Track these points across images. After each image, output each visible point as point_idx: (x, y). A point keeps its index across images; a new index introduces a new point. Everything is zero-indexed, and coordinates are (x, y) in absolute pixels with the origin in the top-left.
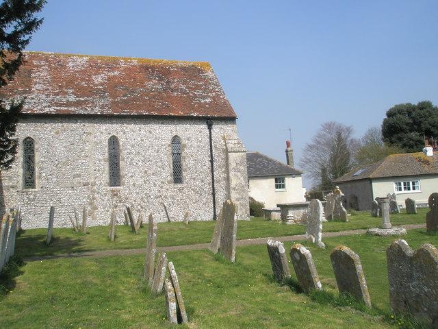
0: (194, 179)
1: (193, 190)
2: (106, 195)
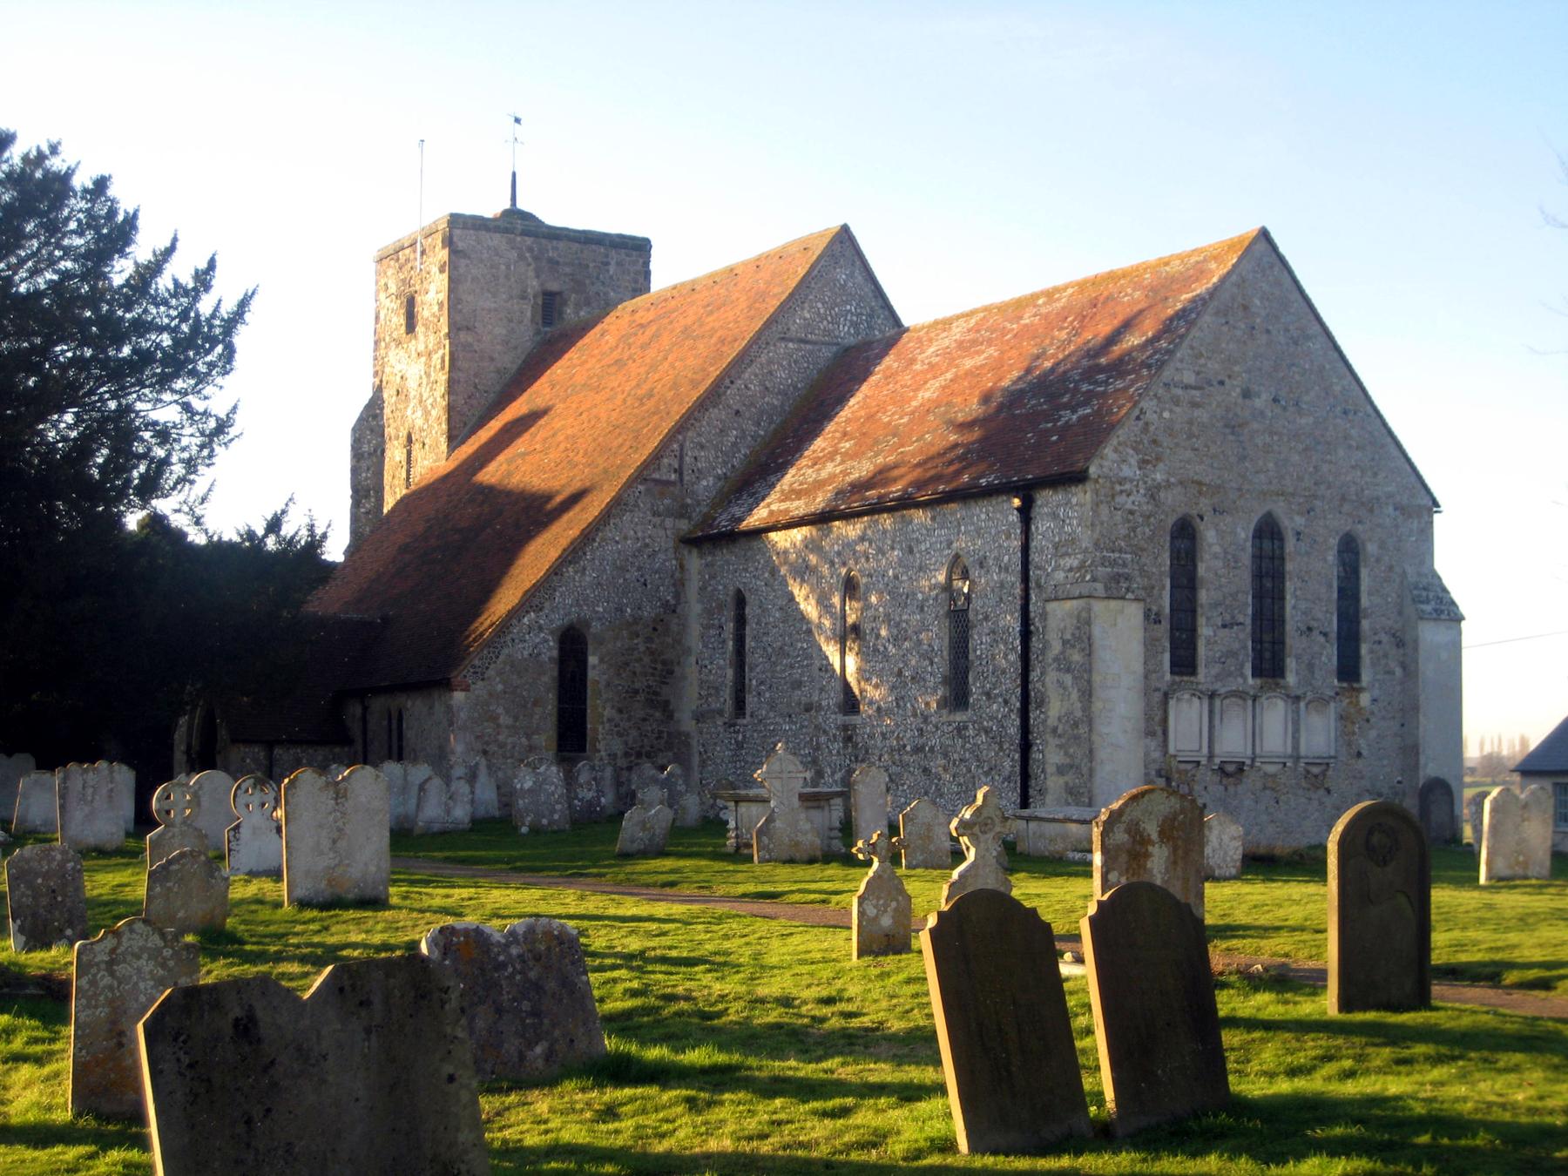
0: (988, 695)
1: (987, 732)
2: (834, 735)
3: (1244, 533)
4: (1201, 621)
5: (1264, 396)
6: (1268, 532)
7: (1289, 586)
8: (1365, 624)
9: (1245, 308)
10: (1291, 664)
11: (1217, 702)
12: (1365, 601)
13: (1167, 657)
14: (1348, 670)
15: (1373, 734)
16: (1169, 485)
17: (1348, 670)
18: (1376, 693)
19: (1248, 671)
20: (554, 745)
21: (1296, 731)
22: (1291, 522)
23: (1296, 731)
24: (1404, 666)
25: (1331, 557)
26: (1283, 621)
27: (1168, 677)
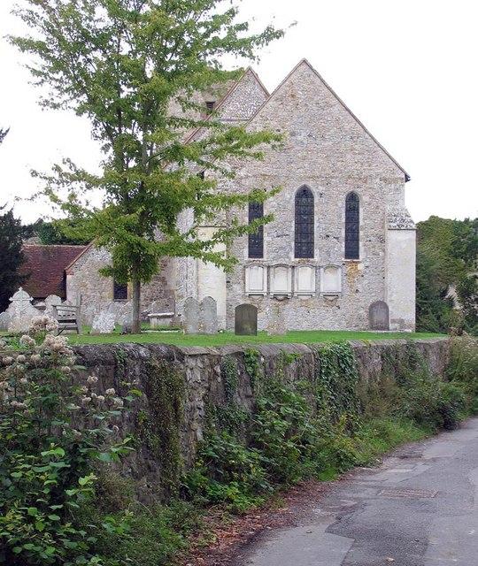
3: (289, 196)
4: (265, 234)
5: (303, 134)
6: (304, 195)
7: (316, 218)
8: (361, 233)
9: (293, 96)
10: (316, 252)
11: (272, 269)
12: (361, 223)
13: (246, 251)
14: (352, 252)
15: (366, 282)
16: (247, 177)
17: (352, 252)
18: (367, 264)
19: (292, 255)
20: (113, 297)
21: (318, 282)
22: (316, 190)
23: (318, 282)
24: (384, 251)
25: (342, 204)
26: (312, 233)
27: (247, 259)
